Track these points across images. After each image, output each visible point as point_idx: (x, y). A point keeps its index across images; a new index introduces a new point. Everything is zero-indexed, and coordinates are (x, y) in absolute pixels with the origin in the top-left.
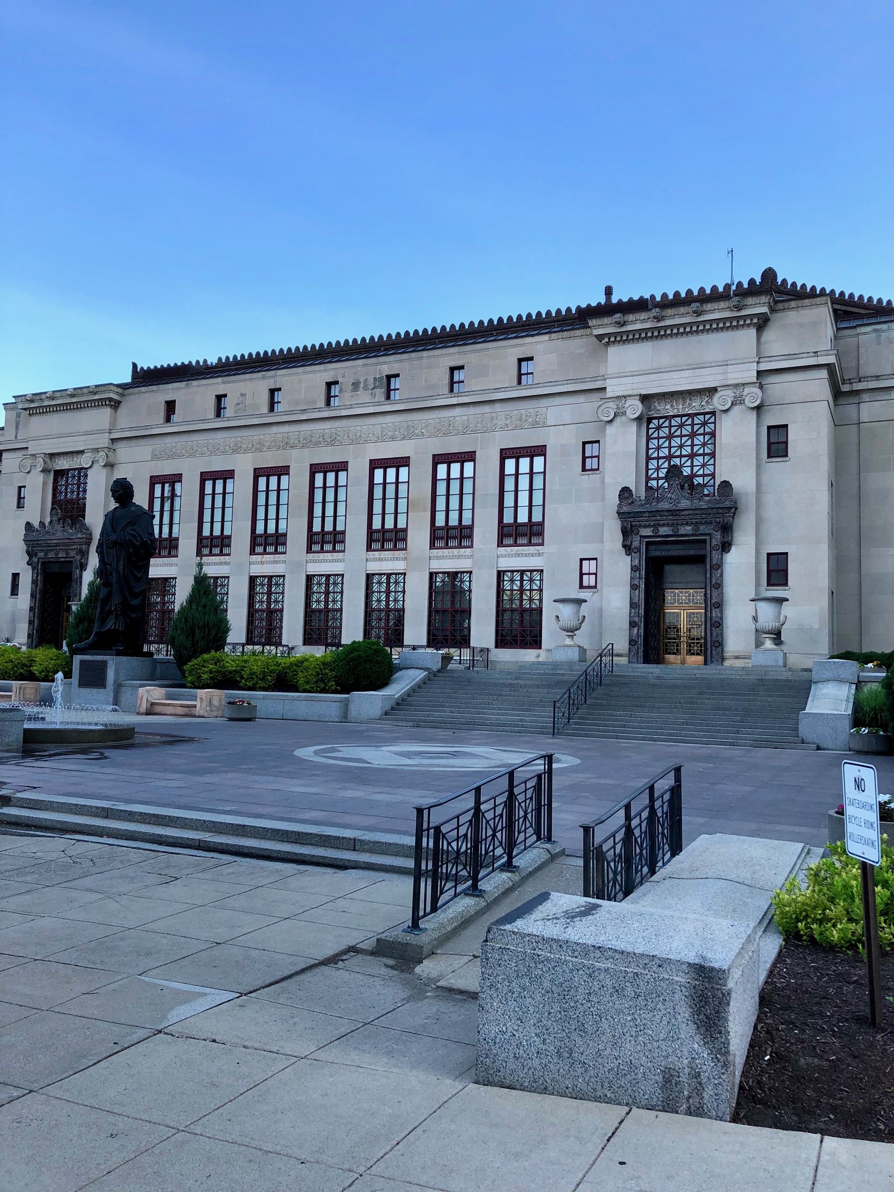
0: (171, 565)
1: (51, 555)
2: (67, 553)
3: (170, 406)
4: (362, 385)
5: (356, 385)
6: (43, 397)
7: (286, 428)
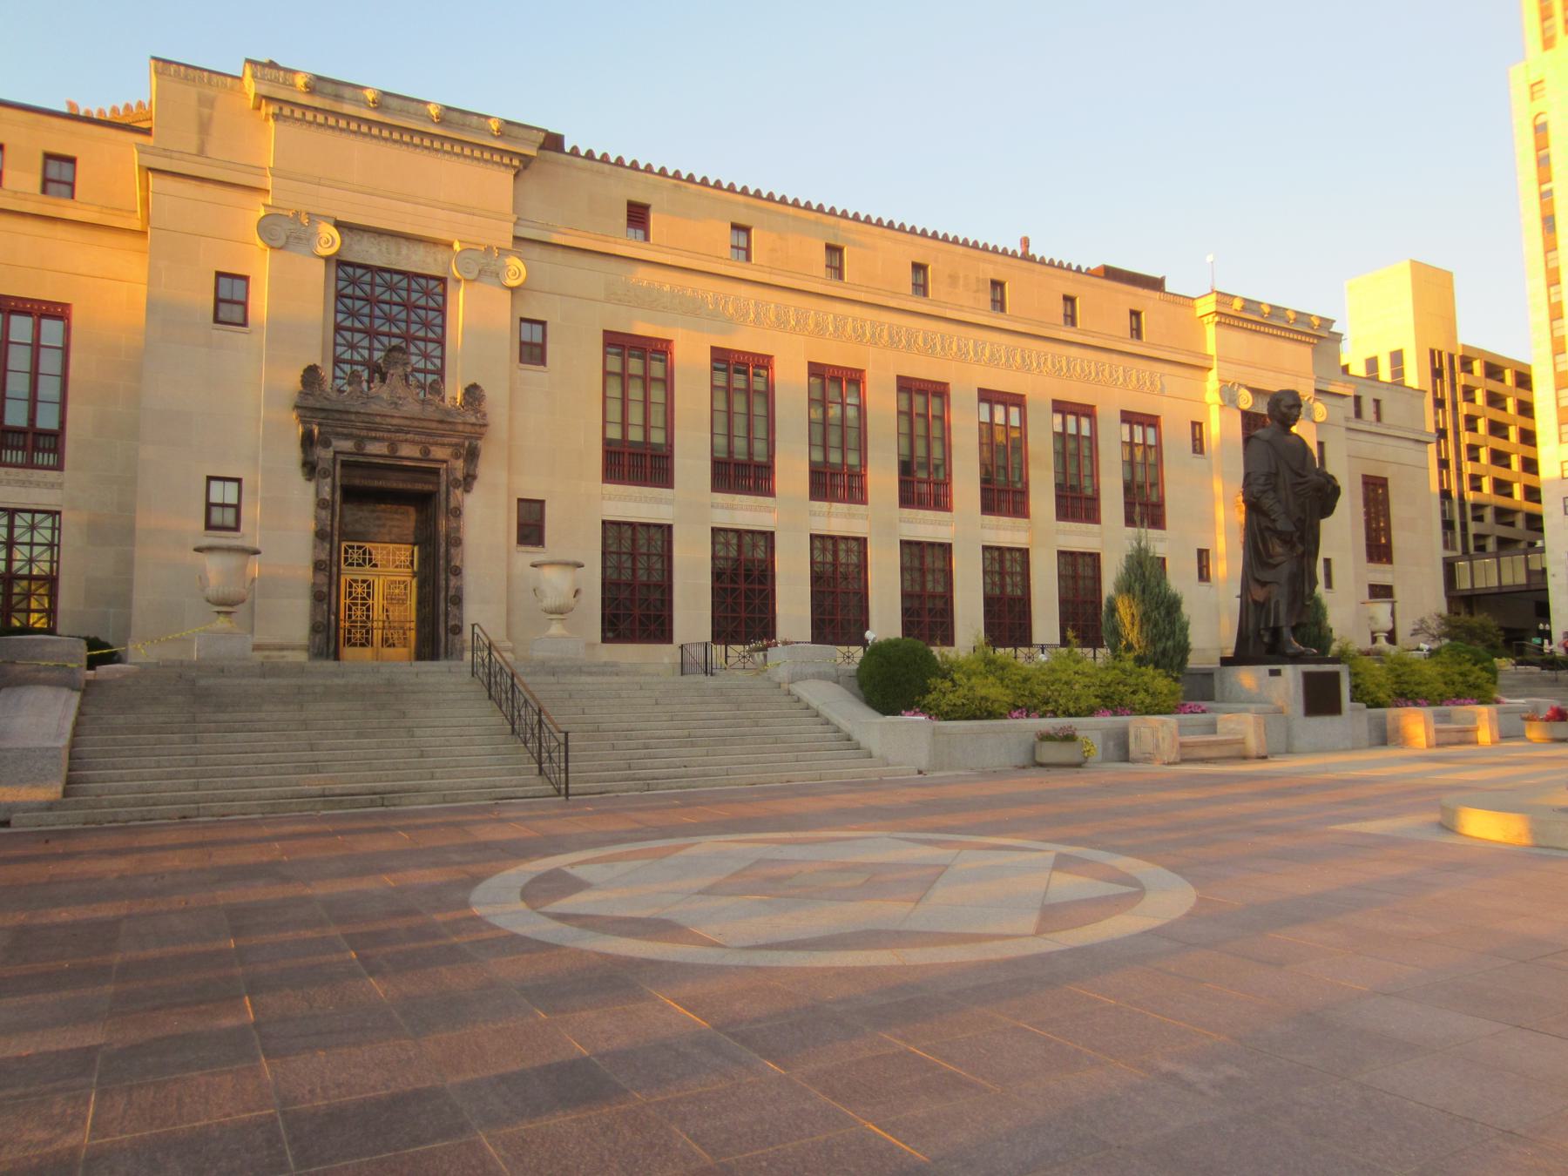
0: (659, 501)
1: (374, 448)
2: (426, 452)
4: (961, 282)
5: (953, 279)
6: (348, 93)
7: (857, 311)
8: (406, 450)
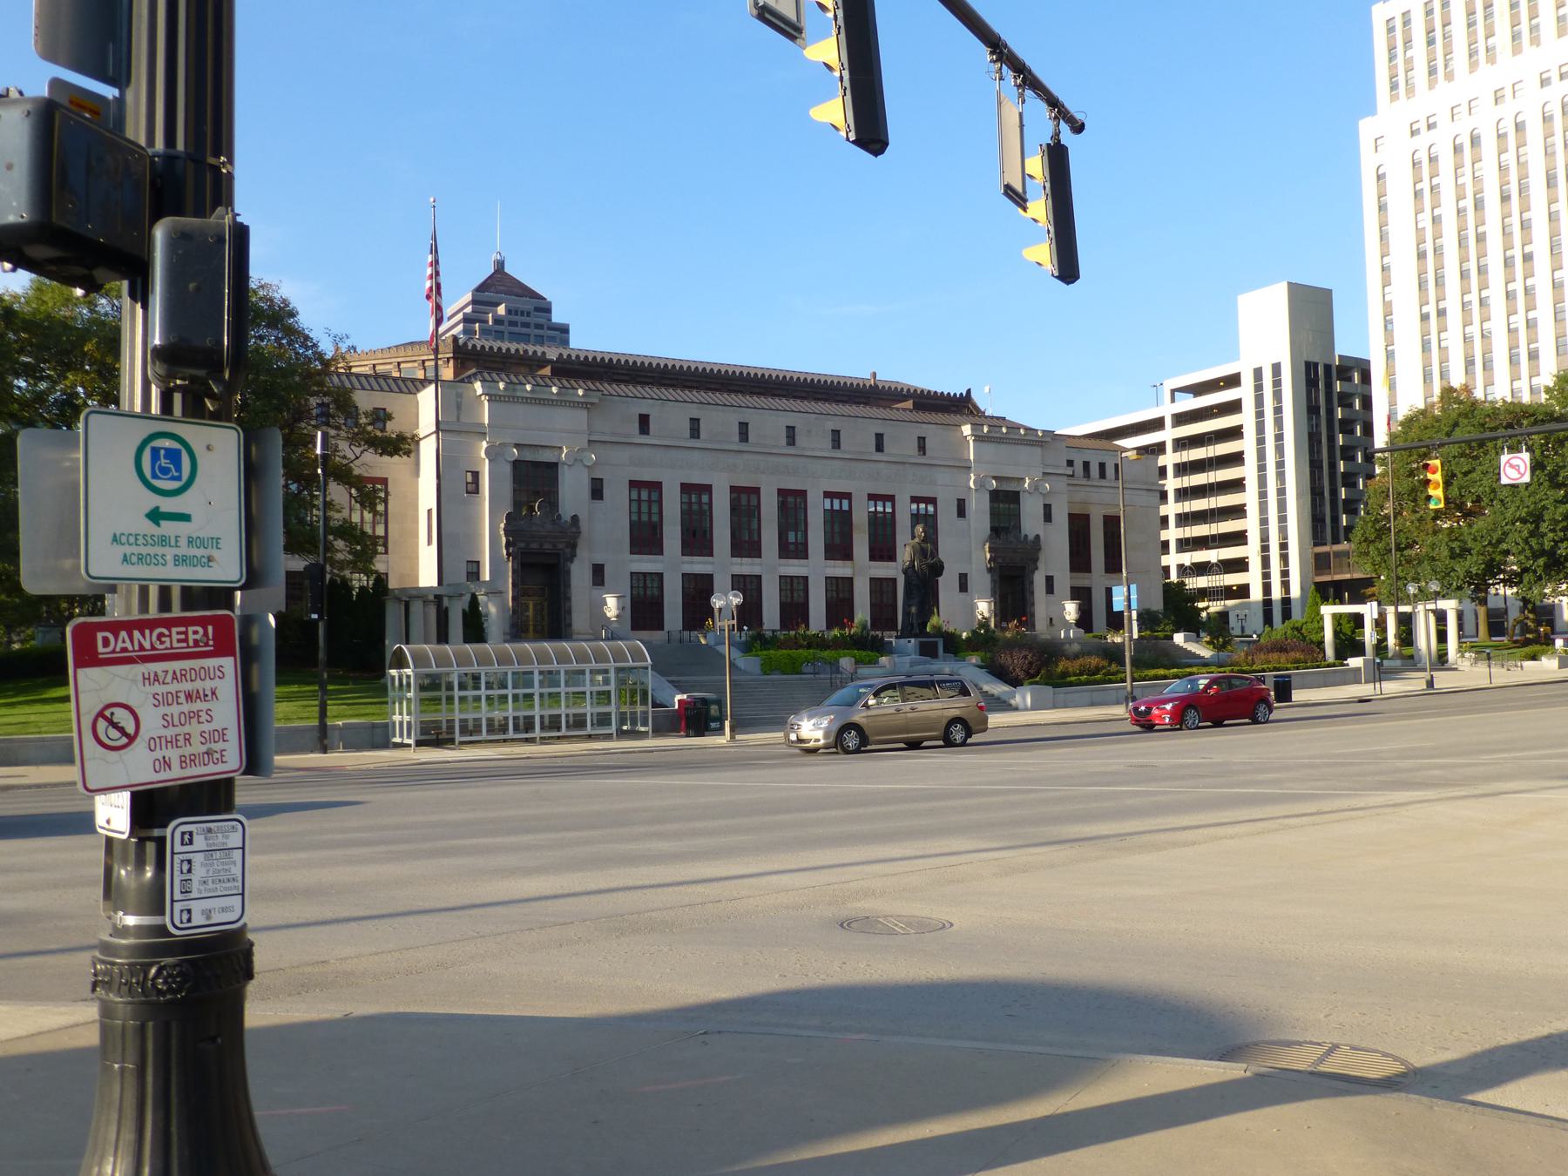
1: (534, 546)
3: (644, 421)
8: (546, 546)
